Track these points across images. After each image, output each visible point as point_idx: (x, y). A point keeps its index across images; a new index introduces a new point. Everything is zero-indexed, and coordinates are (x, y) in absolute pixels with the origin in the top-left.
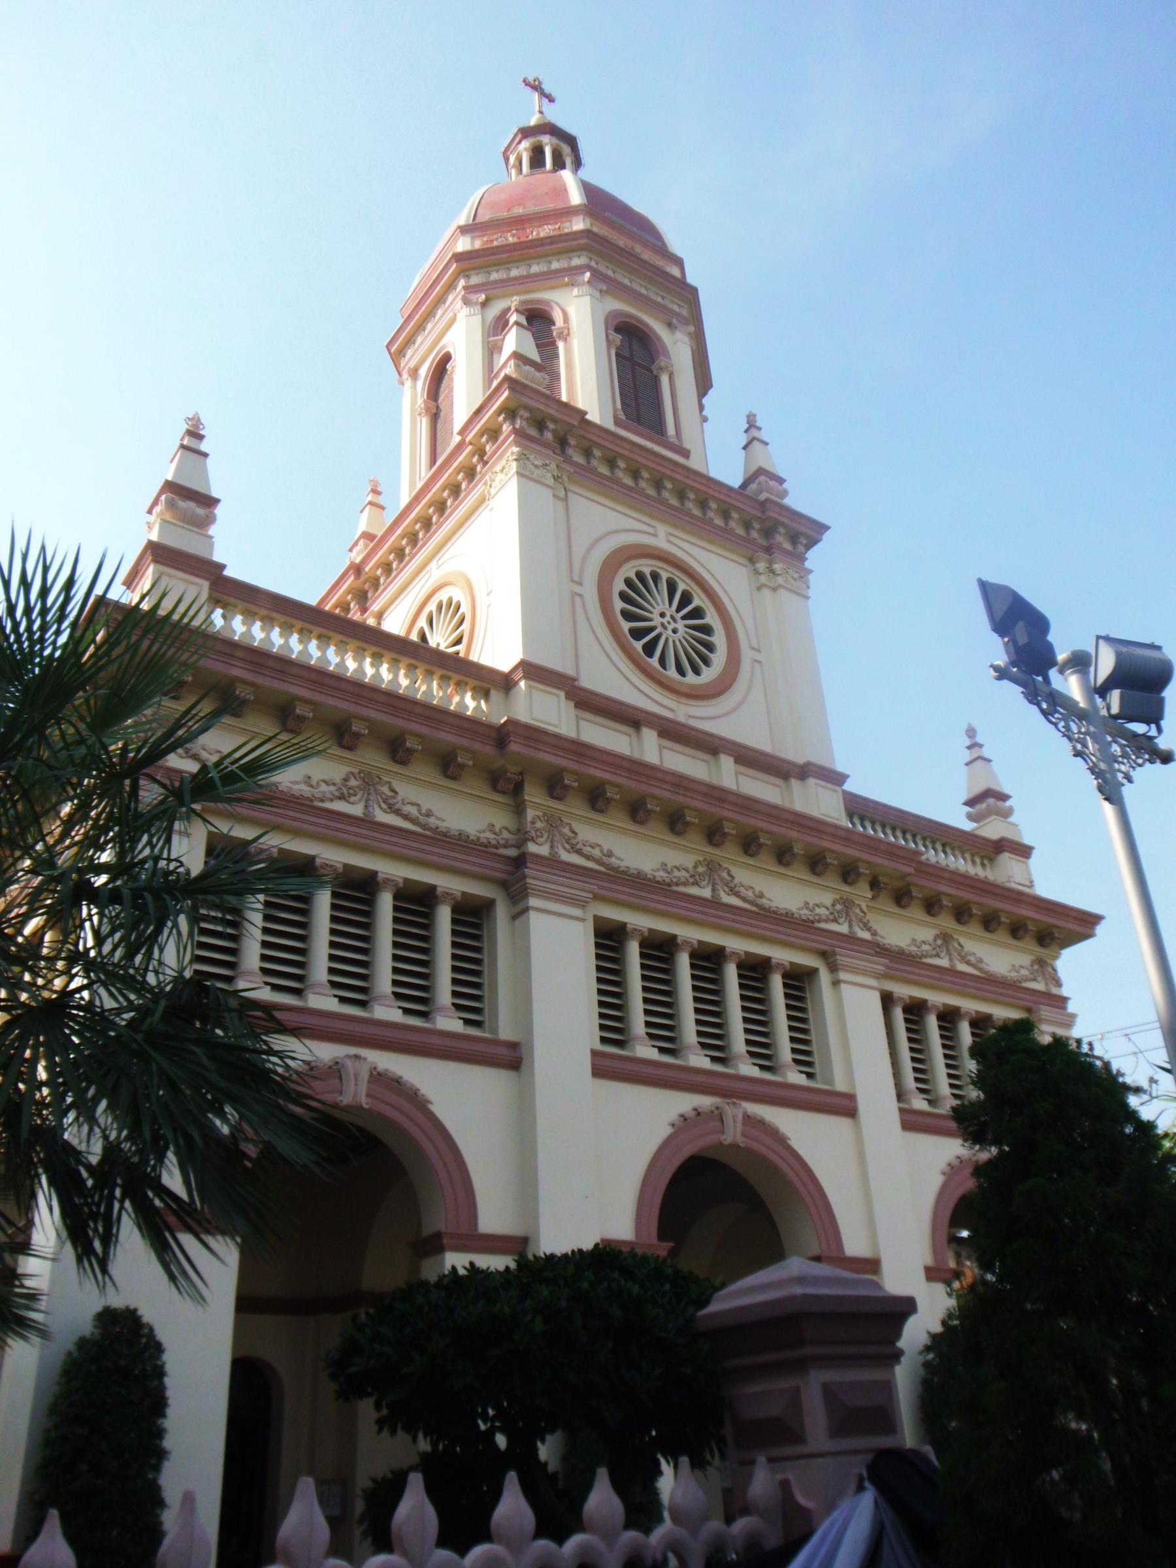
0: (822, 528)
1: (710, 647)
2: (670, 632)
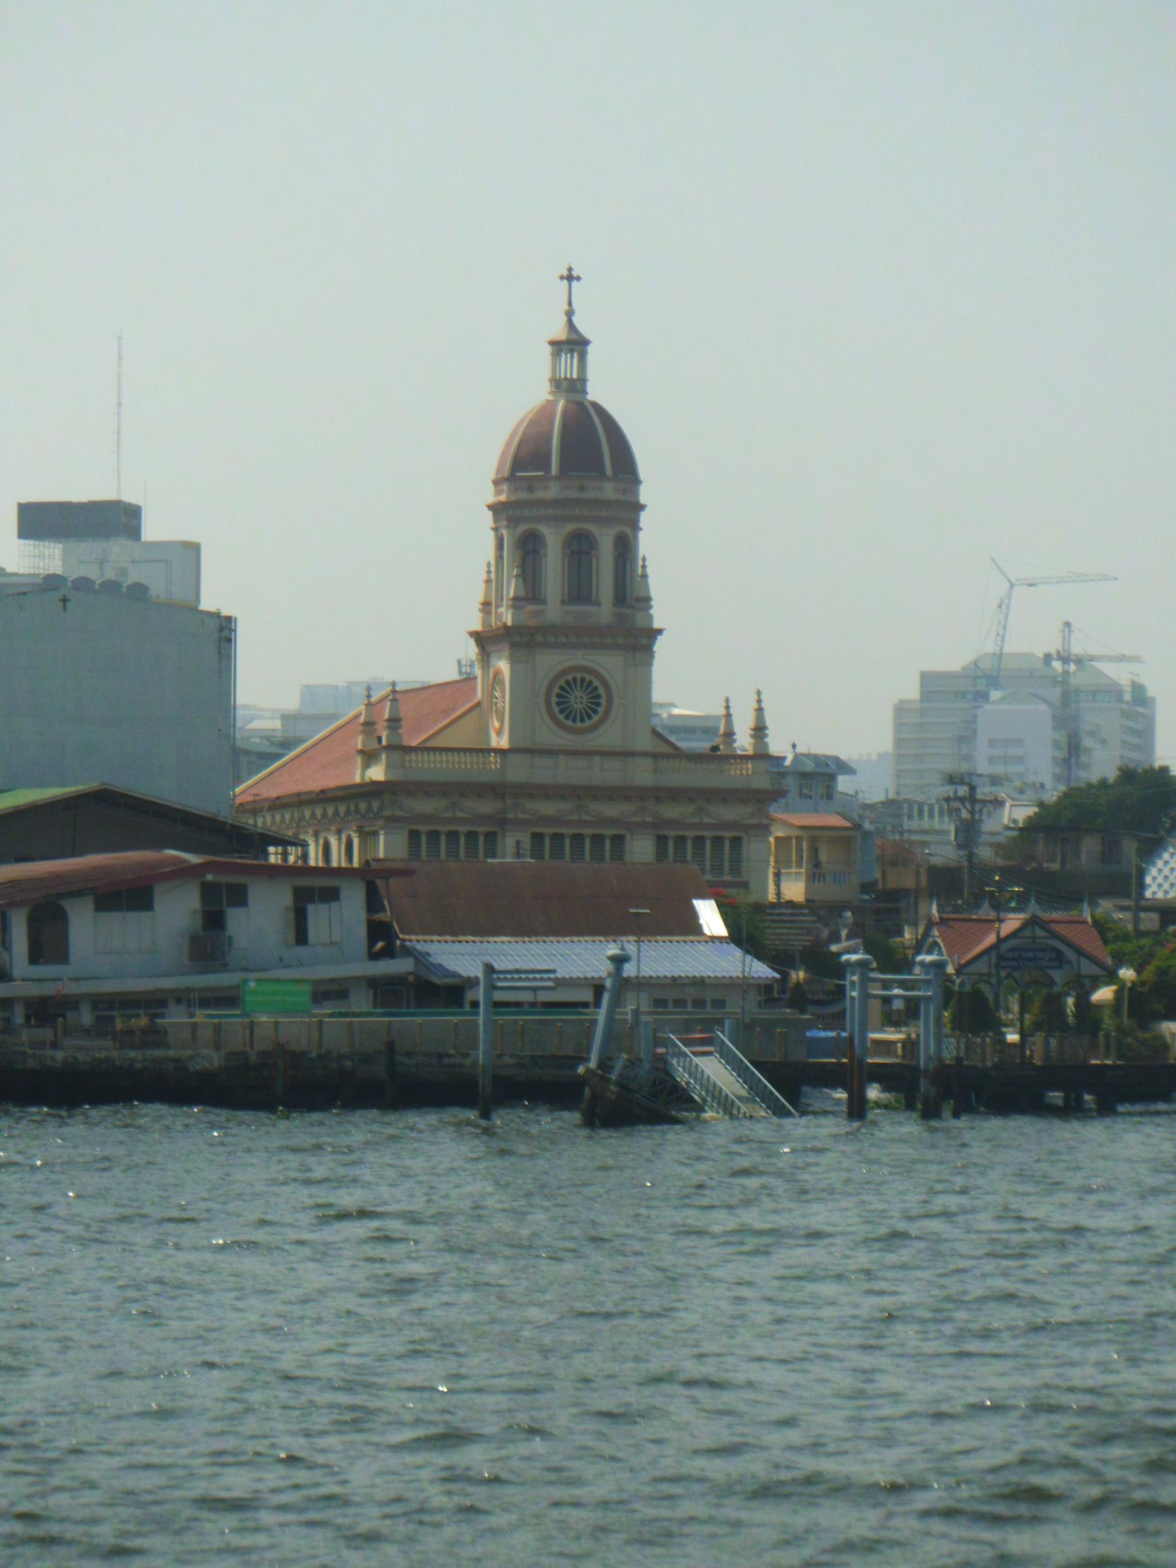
2: (579, 705)
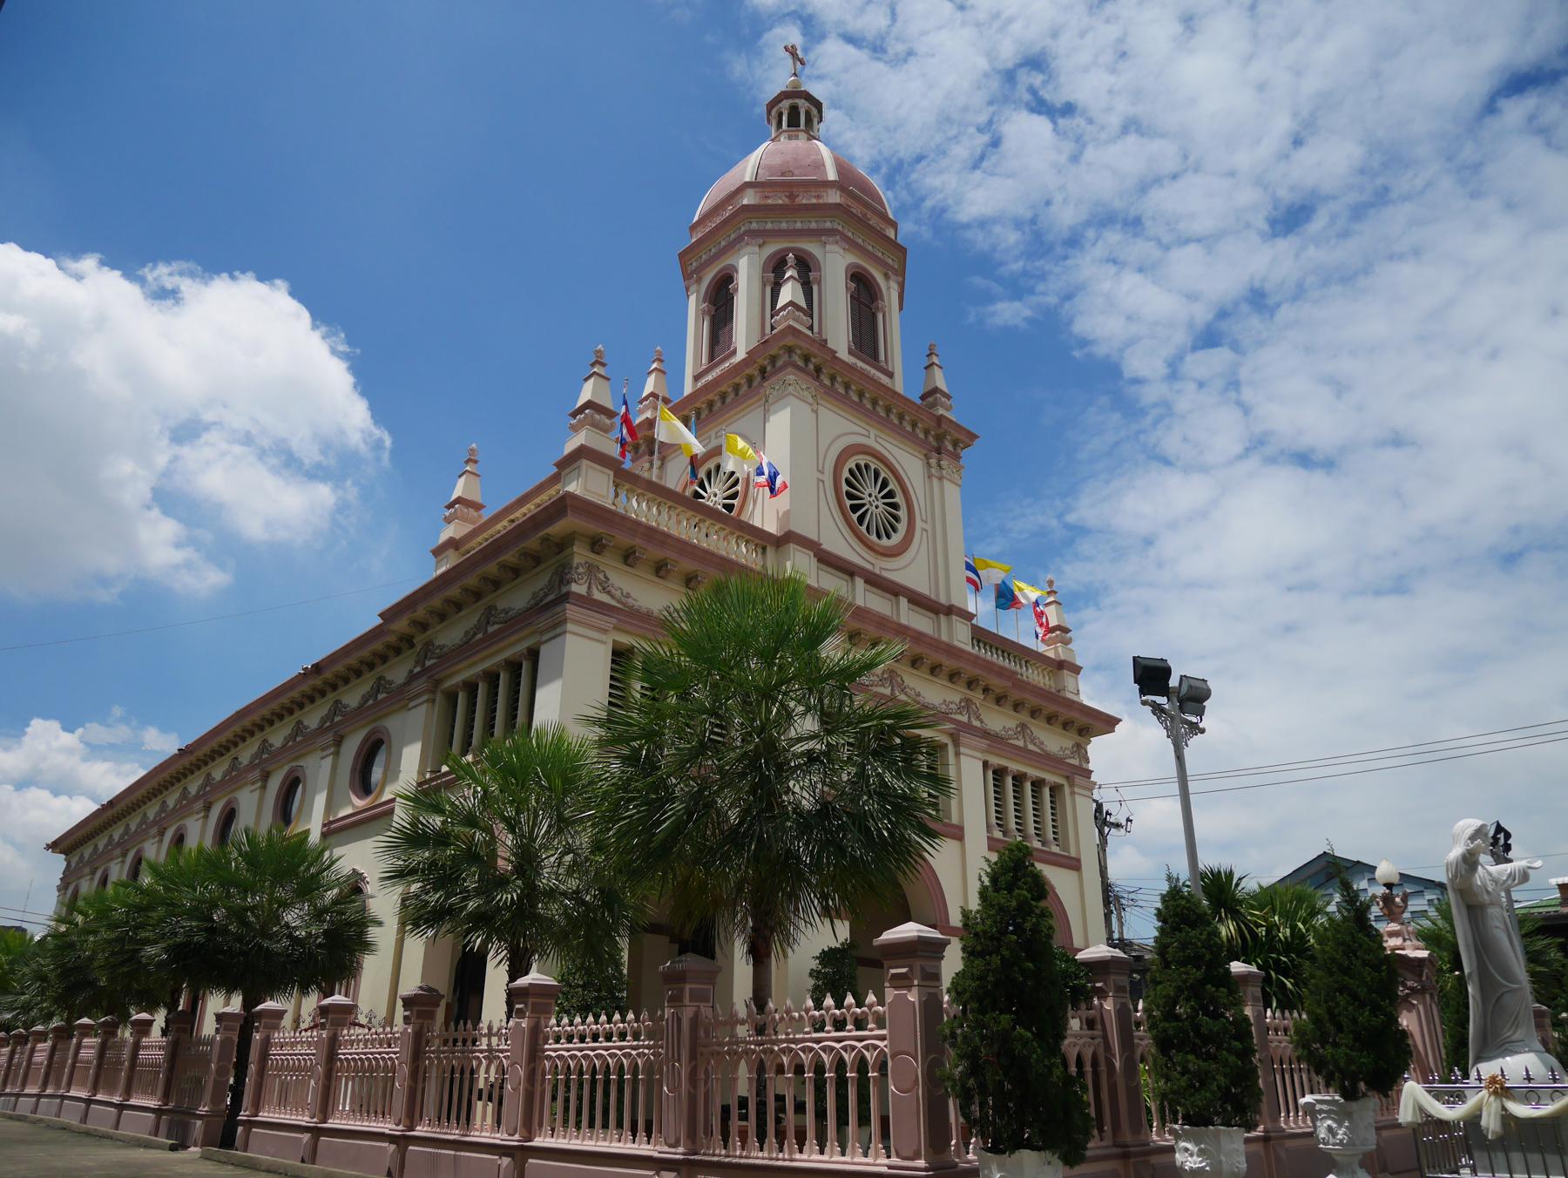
0: (973, 437)
1: (897, 519)
